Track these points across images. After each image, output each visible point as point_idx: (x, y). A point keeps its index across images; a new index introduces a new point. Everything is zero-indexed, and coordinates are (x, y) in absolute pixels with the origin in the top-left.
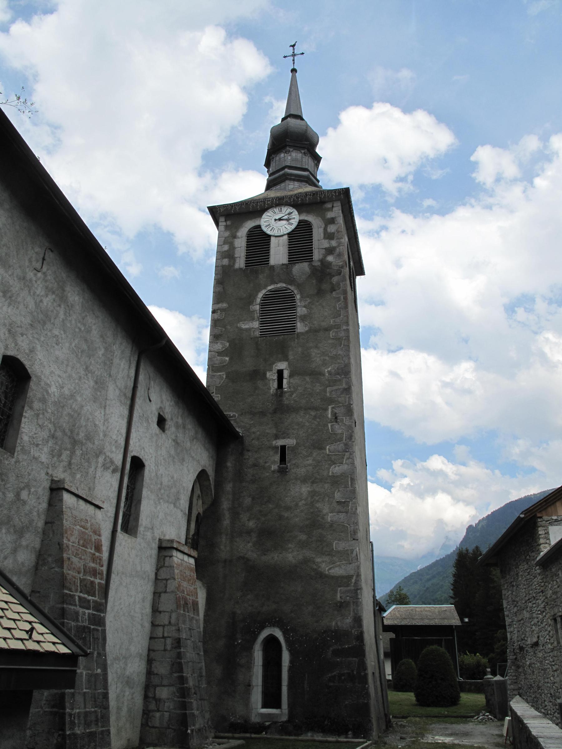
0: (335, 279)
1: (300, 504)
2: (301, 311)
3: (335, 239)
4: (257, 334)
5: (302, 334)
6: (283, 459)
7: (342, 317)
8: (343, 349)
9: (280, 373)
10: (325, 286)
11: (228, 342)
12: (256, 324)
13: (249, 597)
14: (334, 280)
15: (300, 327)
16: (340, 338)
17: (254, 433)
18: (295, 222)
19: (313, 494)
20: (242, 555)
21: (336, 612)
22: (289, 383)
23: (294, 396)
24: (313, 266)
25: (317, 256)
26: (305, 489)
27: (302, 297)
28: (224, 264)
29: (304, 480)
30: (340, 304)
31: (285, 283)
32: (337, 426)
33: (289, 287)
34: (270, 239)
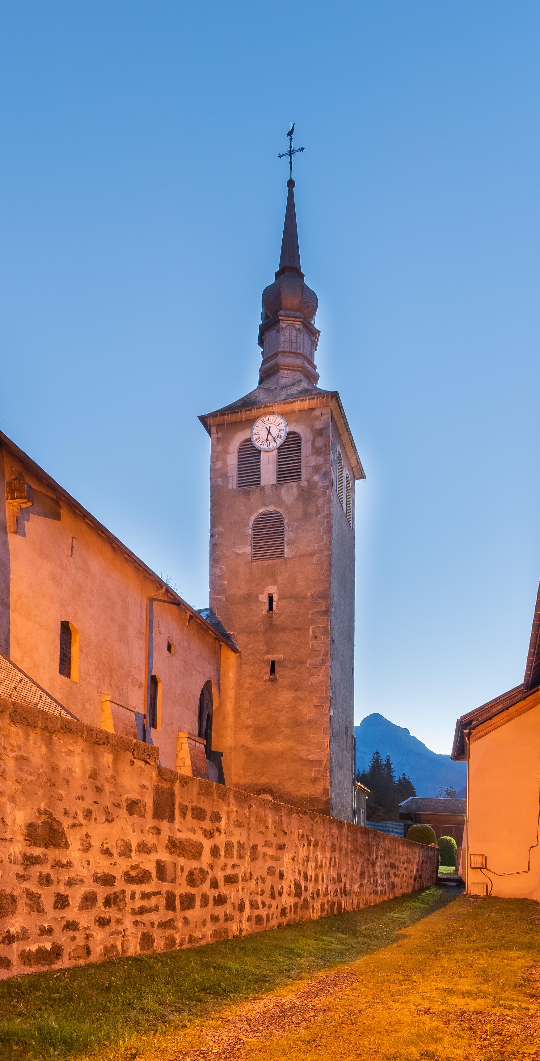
5: (290, 558)
6: (273, 671)
8: (325, 574)
10: (312, 509)
13: (248, 773)
17: (250, 649)
19: (296, 699)
20: (242, 744)
21: (311, 785)
22: (278, 605)
23: (281, 618)
24: (301, 487)
33: (279, 510)
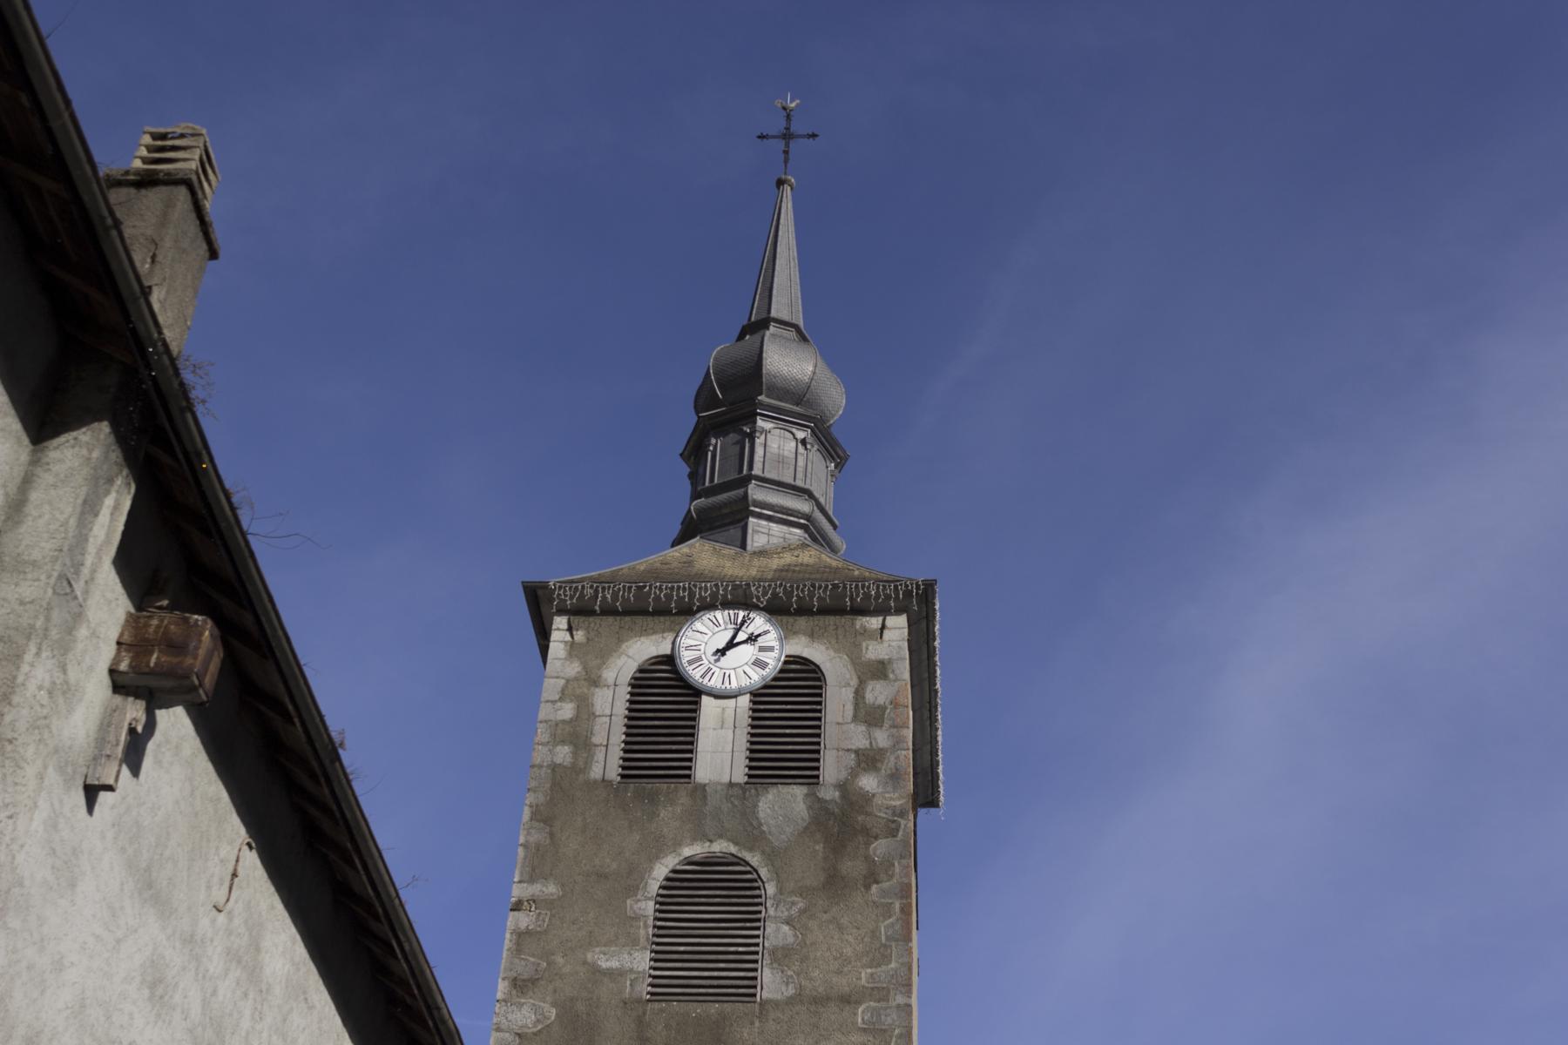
0: (880, 848)
2: (776, 933)
3: (886, 725)
4: (644, 989)
5: (776, 1004)
7: (893, 965)
10: (852, 867)
11: (554, 1004)
12: (641, 961)
14: (875, 849)
15: (771, 984)
16: (885, 1031)
18: (773, 661)
24: (819, 800)
25: (832, 767)
27: (780, 891)
28: (558, 760)
30: (892, 925)
31: (736, 844)
33: (748, 856)
34: (698, 703)
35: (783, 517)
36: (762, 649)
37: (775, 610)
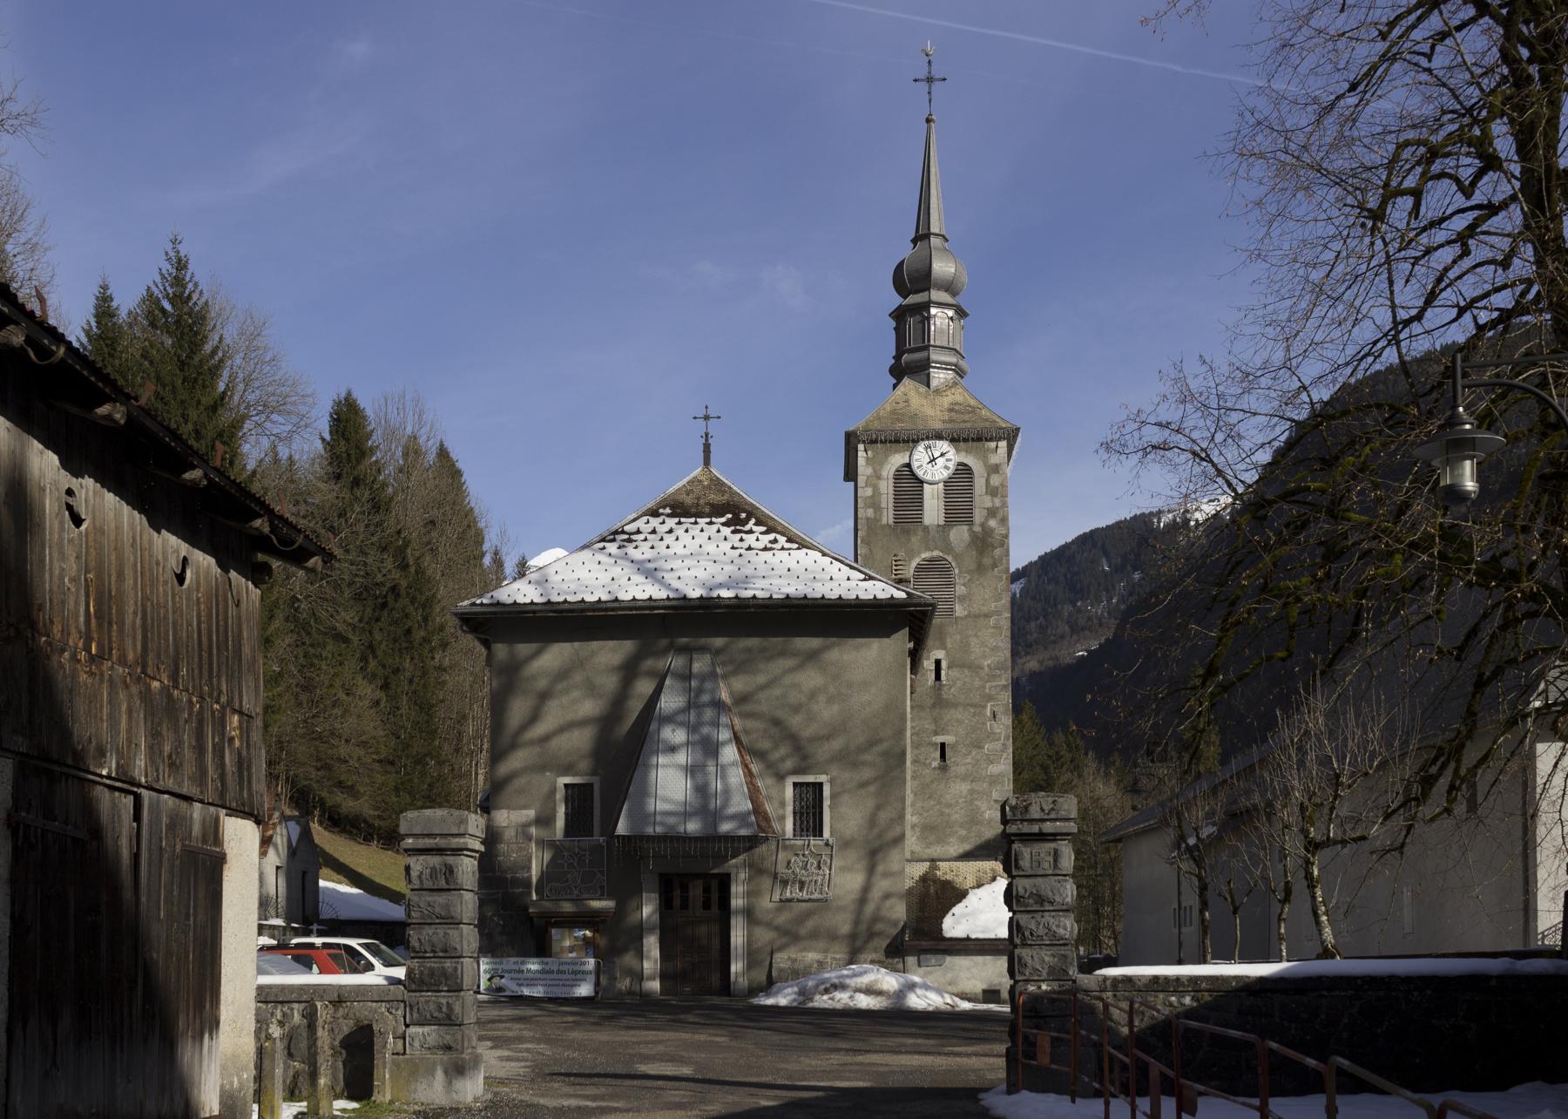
0: (997, 552)
1: (960, 801)
2: (960, 590)
6: (943, 756)
9: (938, 663)
10: (987, 561)
15: (959, 610)
18: (951, 465)
19: (972, 792)
22: (947, 675)
24: (974, 532)
25: (978, 516)
26: (964, 787)
27: (960, 572)
28: (869, 515)
29: (964, 778)
32: (996, 726)
35: (945, 366)
36: (947, 460)
37: (953, 440)
